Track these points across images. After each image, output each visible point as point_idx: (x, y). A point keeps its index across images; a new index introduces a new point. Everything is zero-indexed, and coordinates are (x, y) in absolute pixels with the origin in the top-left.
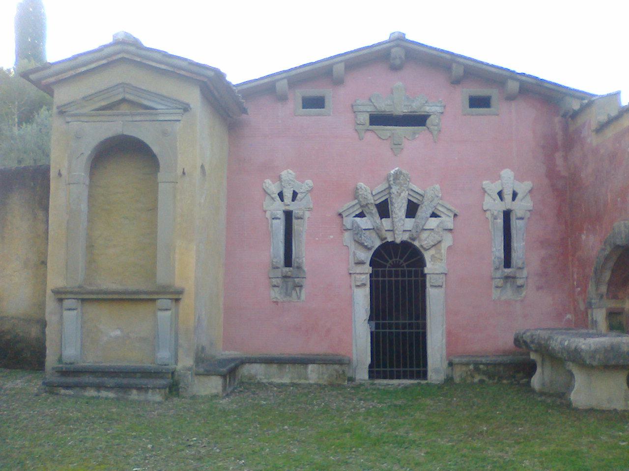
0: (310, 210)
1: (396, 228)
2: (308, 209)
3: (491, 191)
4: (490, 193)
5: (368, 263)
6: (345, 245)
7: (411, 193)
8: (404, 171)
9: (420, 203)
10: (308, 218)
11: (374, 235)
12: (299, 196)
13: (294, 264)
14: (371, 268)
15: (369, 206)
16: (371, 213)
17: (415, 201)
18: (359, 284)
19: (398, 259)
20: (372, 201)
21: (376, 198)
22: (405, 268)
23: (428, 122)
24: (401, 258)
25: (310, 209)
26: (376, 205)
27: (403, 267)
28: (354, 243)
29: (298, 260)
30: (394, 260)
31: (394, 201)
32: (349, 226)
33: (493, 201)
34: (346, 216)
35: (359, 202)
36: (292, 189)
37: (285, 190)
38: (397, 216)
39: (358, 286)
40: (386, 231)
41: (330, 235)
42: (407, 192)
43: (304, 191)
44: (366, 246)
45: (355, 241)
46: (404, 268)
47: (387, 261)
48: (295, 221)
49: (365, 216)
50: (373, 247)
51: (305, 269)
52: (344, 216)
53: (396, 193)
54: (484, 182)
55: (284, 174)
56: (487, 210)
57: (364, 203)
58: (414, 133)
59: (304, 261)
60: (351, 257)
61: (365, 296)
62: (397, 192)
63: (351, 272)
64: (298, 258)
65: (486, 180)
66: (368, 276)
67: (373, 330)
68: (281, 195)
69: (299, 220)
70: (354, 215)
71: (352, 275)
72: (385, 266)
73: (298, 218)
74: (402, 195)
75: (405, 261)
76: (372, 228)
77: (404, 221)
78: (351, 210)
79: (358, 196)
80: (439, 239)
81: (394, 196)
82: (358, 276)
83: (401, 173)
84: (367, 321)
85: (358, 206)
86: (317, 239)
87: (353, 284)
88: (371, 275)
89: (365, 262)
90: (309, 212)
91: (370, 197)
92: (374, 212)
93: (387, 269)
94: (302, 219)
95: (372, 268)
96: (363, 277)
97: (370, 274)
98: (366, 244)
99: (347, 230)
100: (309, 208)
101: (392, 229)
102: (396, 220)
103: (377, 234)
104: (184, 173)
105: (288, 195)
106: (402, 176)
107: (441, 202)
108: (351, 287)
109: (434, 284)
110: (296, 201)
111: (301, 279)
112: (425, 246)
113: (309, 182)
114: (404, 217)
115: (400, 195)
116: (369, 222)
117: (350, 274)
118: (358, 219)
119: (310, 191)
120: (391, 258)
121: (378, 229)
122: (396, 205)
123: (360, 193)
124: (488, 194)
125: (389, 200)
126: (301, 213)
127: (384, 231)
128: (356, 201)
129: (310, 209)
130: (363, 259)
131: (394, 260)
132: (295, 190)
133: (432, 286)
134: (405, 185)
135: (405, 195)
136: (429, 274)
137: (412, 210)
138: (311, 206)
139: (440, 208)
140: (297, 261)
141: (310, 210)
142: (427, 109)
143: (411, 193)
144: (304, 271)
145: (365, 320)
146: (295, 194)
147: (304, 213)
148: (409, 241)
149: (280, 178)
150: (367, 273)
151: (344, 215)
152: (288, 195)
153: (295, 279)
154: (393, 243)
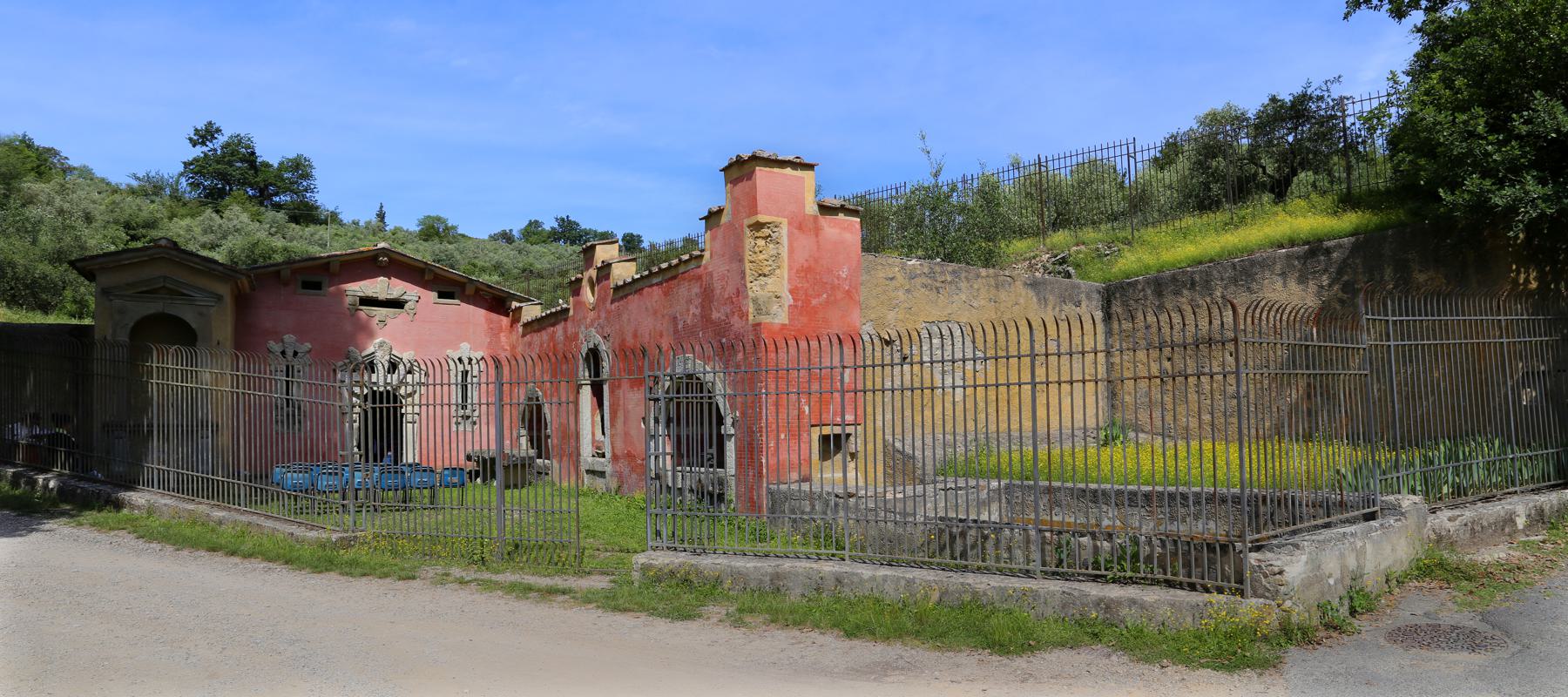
8: (386, 341)
23: (406, 306)
37: (287, 350)
55: (286, 337)
58: (395, 314)
68: (283, 353)
83: (385, 342)
91: (360, 358)
104: (218, 343)
105: (290, 353)
113: (308, 345)
119: (309, 352)
135: (387, 357)
137: (393, 367)
142: (405, 297)
146: (295, 354)
149: (282, 341)
152: (290, 353)
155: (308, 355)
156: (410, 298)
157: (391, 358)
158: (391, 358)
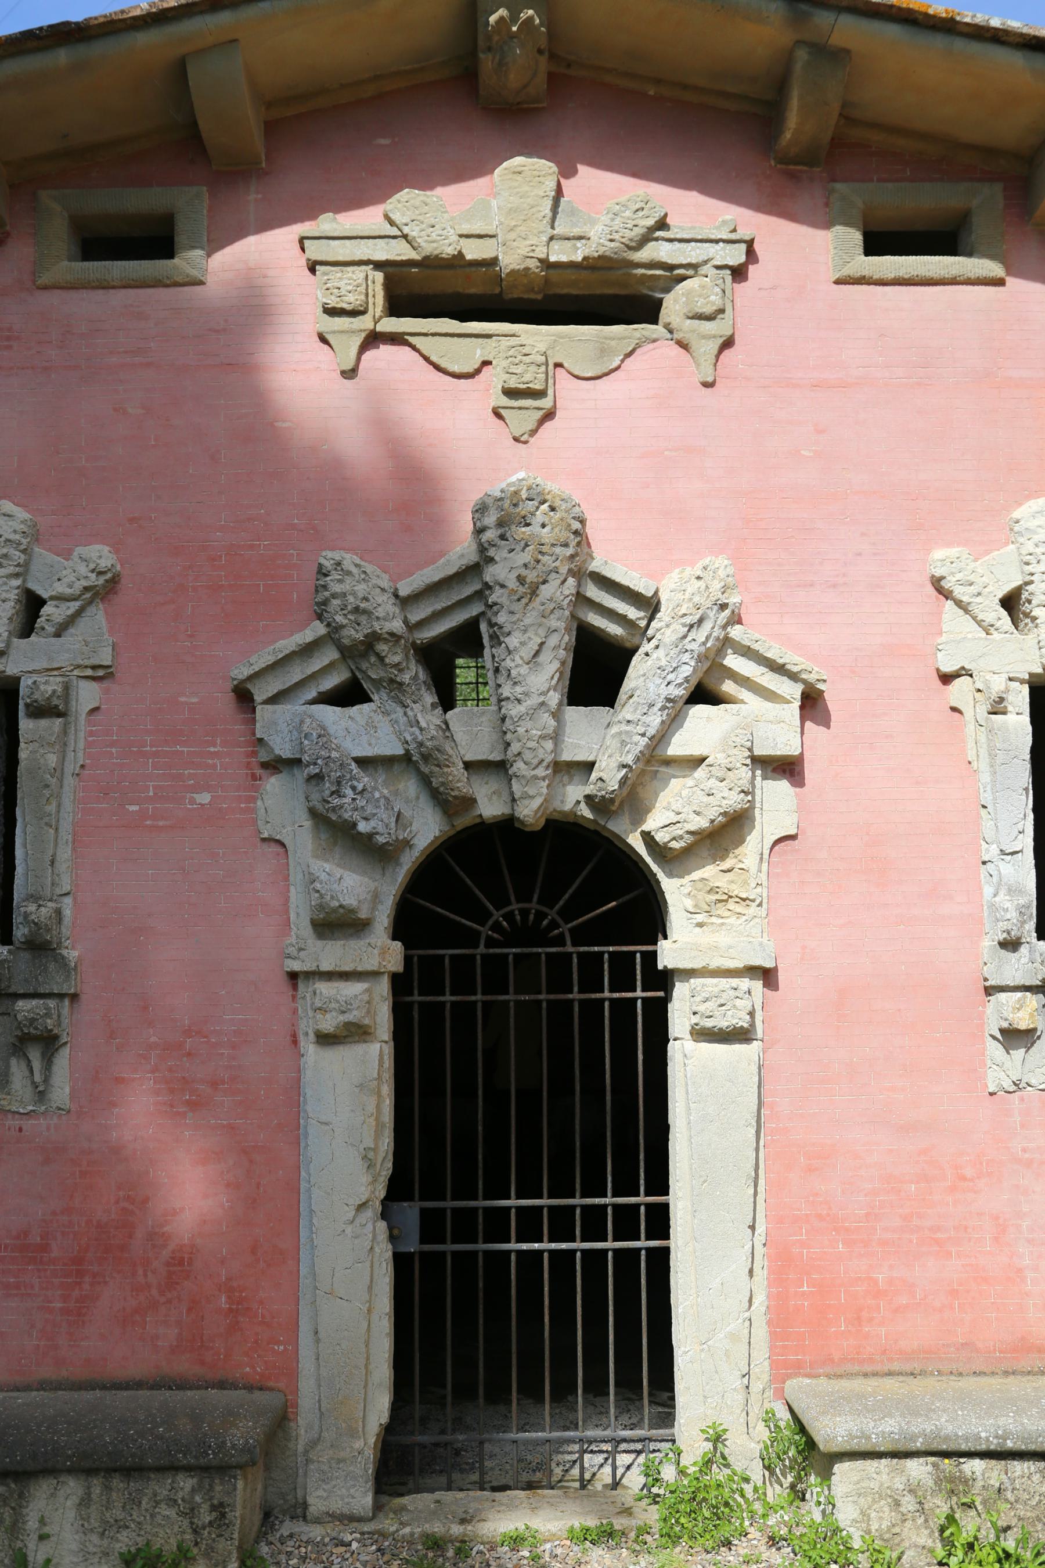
0: (102, 674)
1: (515, 748)
2: (89, 672)
3: (973, 589)
4: (965, 599)
5: (383, 918)
6: (266, 835)
7: (593, 592)
9: (636, 641)
10: (95, 710)
11: (410, 786)
12: (46, 610)
13: (20, 932)
14: (398, 945)
15: (382, 648)
16: (395, 686)
17: (615, 630)
18: (329, 1023)
19: (534, 905)
20: (397, 625)
21: (416, 615)
22: (570, 949)
24: (548, 900)
25: (101, 673)
26: (414, 645)
27: (560, 941)
28: (308, 824)
29: (32, 908)
30: (515, 906)
31: (501, 618)
32: (283, 748)
33: (984, 634)
34: (273, 700)
35: (334, 630)
36: (17, 582)
38: (518, 689)
39: (325, 1039)
40: (468, 765)
41: (197, 789)
42: (571, 581)
43: (68, 591)
44: (370, 836)
45: (313, 813)
46: (564, 945)
47: (483, 917)
48: (26, 725)
49: (370, 700)
50: (407, 844)
51: (72, 955)
52: (258, 698)
53: (512, 583)
54: (938, 554)
56: (956, 675)
57: (353, 634)
59: (67, 912)
60: (296, 896)
61: (361, 1086)
62: (521, 580)
63: (296, 966)
64: (34, 898)
65: (949, 545)
66: (384, 987)
67: (412, 1246)
69: (44, 723)
70: (312, 694)
71: (301, 986)
72: (471, 939)
73: (39, 711)
74: (546, 591)
75: (567, 914)
76: (402, 752)
77: (557, 715)
78: (296, 674)
79: (325, 603)
80: (733, 801)
81: (504, 600)
82: (324, 988)
84: (369, 1214)
85: (330, 654)
86: (134, 808)
87: (307, 1027)
88: (400, 983)
89: (363, 915)
90: (94, 685)
91: (385, 606)
92: (406, 678)
93: (482, 949)
94: (60, 715)
95: (407, 946)
96: (354, 989)
97: (395, 978)
98: (363, 827)
99: (277, 765)
100: (94, 668)
101: (495, 756)
102: (514, 710)
103: (425, 781)
106: (545, 507)
107: (736, 632)
108: (295, 1042)
109: (709, 1023)
110: (33, 638)
111: (52, 1003)
112: (661, 837)
113: (102, 555)
114: (554, 698)
115: (534, 592)
116: (385, 729)
117: (293, 976)
118: (329, 714)
120: (500, 902)
121: (426, 758)
122: (512, 641)
123: (337, 588)
124: (959, 603)
125: (483, 627)
126: (50, 686)
127: (457, 770)
128: (318, 629)
129: (101, 673)
130: (350, 901)
131: (515, 906)
132: (32, 586)
133: (704, 1035)
134: (558, 550)
136: (689, 974)
138: (105, 657)
139: (732, 661)
140: (26, 915)
141: (102, 674)
143: (593, 592)
144: (63, 963)
145: (361, 1207)
147: (67, 687)
148: (586, 812)
150: (375, 974)
151: (261, 692)
153: (21, 1004)
154: (508, 825)
155: (97, 617)
156: (692, 254)
157: (581, 599)
158: (581, 599)
